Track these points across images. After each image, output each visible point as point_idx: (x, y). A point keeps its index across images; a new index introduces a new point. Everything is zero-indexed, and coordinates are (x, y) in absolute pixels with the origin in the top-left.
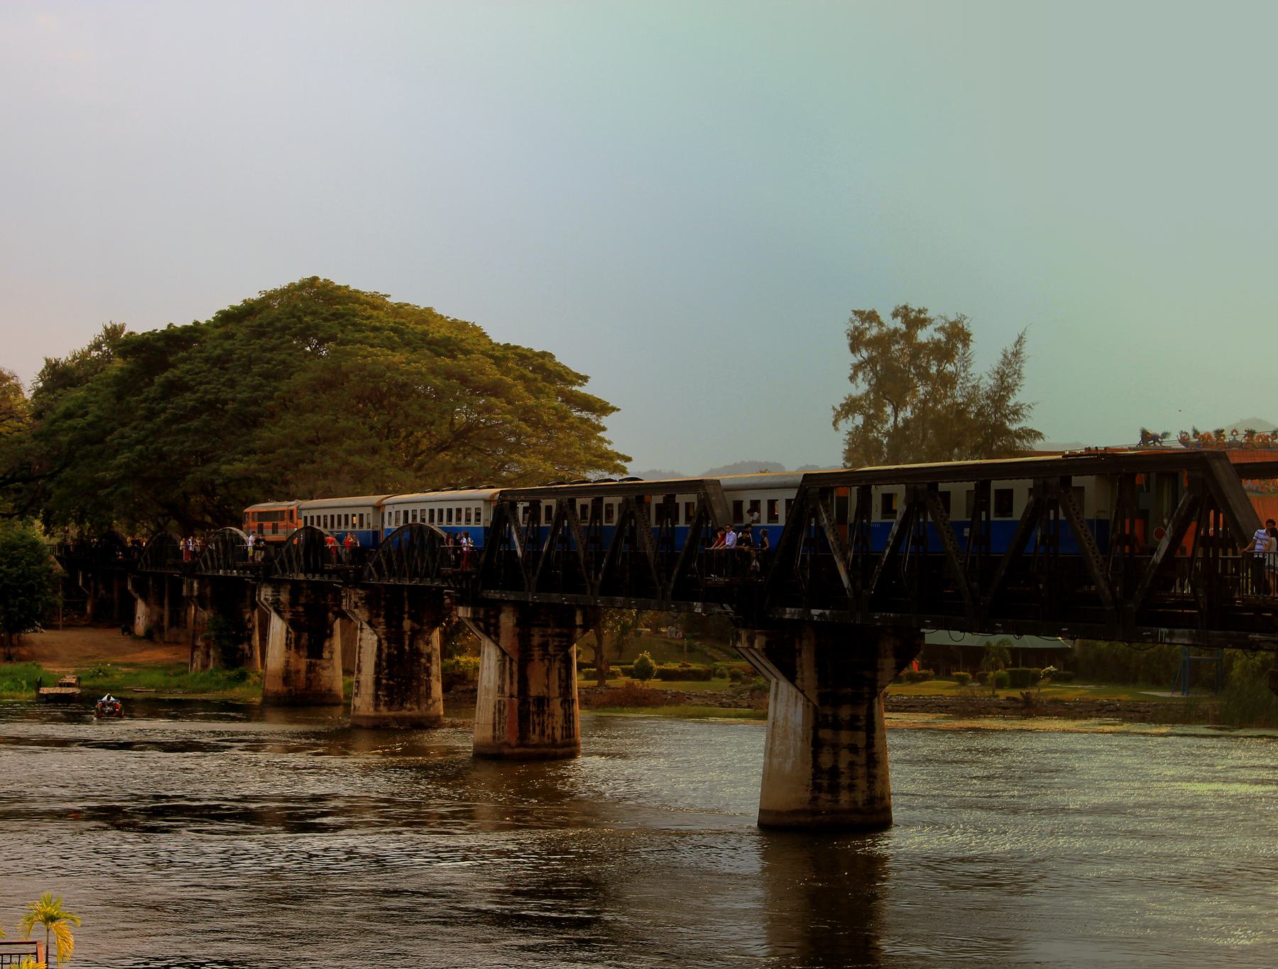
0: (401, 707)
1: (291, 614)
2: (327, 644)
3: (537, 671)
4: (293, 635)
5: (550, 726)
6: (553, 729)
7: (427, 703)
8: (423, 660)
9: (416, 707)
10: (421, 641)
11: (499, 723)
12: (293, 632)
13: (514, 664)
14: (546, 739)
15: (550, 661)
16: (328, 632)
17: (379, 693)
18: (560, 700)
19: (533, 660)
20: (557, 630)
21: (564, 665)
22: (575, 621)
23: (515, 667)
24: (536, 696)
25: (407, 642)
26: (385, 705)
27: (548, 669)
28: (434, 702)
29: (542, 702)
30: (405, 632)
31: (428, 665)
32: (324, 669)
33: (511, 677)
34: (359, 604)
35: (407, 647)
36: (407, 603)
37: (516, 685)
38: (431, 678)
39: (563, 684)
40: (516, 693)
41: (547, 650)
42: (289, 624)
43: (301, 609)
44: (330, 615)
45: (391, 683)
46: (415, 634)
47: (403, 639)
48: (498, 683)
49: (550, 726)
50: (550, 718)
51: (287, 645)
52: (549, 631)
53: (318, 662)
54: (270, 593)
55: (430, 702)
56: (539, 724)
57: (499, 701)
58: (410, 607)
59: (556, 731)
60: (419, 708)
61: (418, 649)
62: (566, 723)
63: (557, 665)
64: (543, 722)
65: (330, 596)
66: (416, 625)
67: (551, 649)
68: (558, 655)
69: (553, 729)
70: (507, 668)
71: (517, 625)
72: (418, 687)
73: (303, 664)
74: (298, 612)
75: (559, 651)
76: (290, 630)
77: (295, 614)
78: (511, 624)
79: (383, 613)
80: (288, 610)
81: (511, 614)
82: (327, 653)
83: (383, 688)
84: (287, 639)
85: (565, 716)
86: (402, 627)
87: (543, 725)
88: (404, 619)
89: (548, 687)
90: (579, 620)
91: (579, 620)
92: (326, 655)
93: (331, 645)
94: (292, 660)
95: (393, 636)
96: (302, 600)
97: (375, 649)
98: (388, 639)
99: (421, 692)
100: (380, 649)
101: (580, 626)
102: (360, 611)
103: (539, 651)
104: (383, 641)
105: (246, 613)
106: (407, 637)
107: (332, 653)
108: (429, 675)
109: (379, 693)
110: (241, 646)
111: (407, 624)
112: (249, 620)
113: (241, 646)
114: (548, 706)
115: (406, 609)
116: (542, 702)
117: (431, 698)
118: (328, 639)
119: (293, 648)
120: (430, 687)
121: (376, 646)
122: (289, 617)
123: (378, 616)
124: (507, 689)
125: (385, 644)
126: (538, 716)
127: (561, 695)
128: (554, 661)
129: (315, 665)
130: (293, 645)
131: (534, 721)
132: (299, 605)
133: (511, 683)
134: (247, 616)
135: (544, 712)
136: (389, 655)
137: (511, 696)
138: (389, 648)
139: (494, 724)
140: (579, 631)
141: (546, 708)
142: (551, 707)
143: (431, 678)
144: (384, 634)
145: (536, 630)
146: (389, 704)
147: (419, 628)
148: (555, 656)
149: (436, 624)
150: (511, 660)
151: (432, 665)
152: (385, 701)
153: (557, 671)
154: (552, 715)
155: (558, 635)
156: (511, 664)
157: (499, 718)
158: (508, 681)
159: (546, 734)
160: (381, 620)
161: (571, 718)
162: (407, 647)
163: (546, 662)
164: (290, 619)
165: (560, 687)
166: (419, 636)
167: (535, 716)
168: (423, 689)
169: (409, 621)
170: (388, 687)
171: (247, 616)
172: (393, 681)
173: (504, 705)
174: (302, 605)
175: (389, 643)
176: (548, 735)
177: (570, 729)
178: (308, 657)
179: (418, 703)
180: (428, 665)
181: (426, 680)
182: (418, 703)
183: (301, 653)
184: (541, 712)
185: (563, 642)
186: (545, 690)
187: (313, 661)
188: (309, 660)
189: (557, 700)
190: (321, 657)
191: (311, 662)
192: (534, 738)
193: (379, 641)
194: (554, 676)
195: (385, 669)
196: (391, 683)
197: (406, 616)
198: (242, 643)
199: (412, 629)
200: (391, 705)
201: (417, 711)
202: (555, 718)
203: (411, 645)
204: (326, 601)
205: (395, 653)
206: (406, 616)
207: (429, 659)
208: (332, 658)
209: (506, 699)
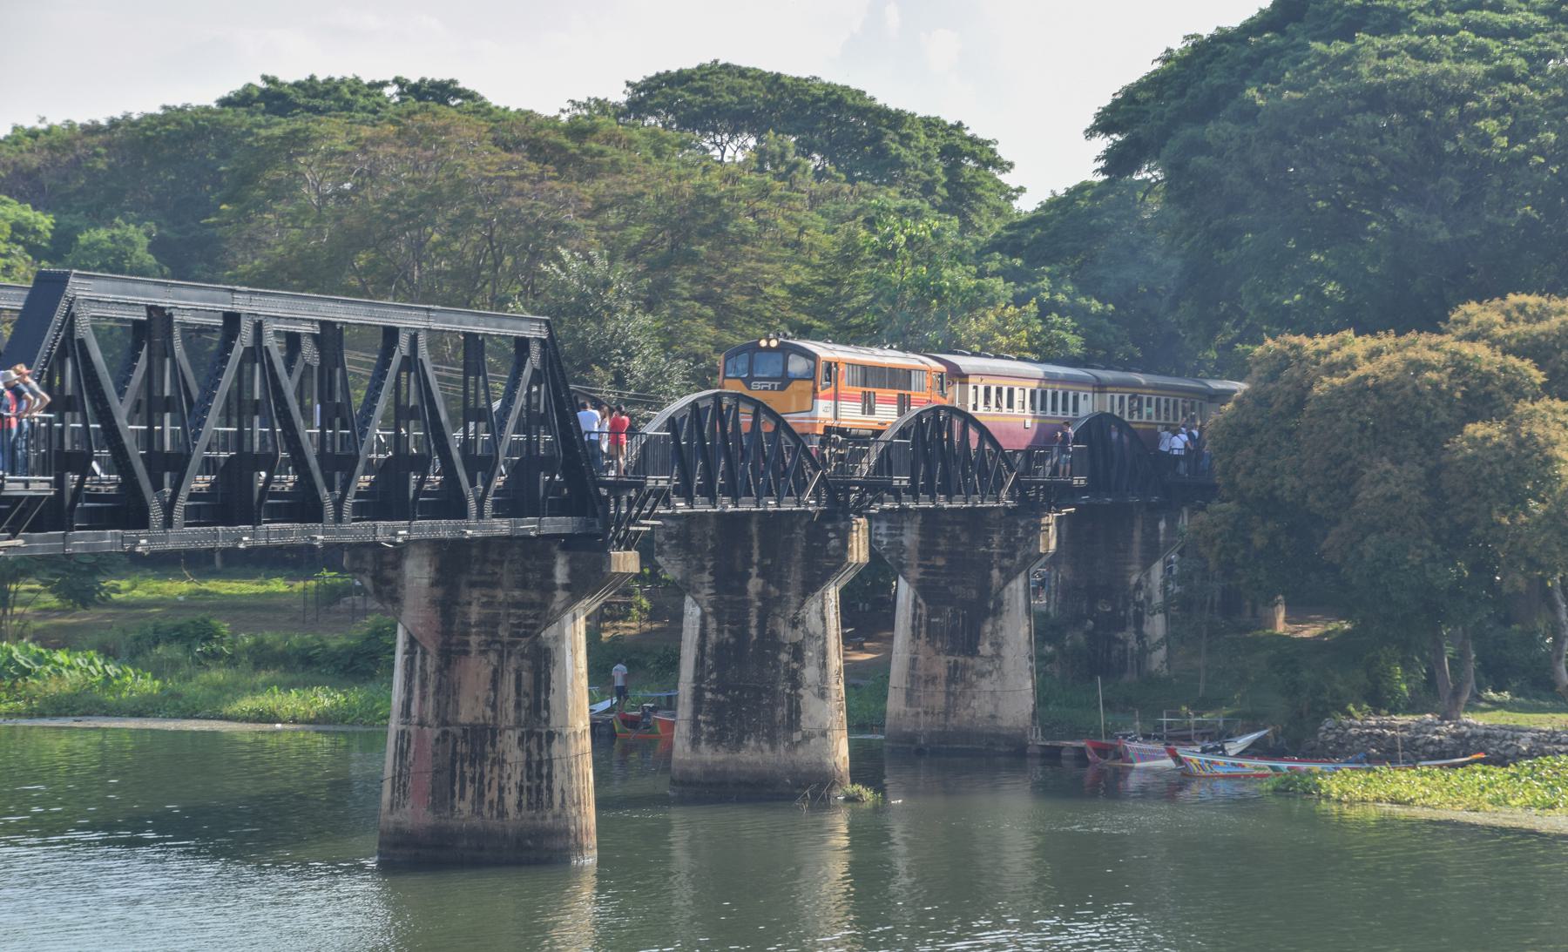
0: (738, 744)
1: (921, 570)
2: (988, 628)
3: (475, 671)
4: (924, 611)
5: (495, 784)
6: (501, 789)
7: (789, 739)
8: (784, 657)
9: (766, 747)
10: (780, 620)
11: (400, 776)
12: (924, 605)
13: (429, 659)
14: (485, 809)
15: (501, 656)
16: (991, 605)
17: (700, 717)
18: (518, 733)
19: (467, 653)
20: (517, 593)
21: (527, 663)
22: (551, 575)
23: (431, 666)
24: (471, 724)
25: (754, 621)
26: (708, 741)
27: (495, 671)
28: (807, 738)
29: (482, 736)
30: (751, 601)
31: (795, 665)
32: (982, 675)
33: (423, 685)
34: (665, 547)
35: (754, 632)
36: (756, 544)
37: (430, 703)
38: (801, 691)
39: (526, 702)
40: (430, 717)
41: (494, 634)
42: (917, 589)
43: (940, 562)
44: (995, 573)
45: (721, 697)
46: (770, 605)
47: (747, 614)
48: (403, 696)
49: (495, 784)
50: (496, 769)
51: (913, 628)
52: (500, 595)
53: (970, 661)
54: (883, 531)
55: (797, 736)
56: (473, 780)
57: (403, 732)
58: (763, 555)
59: (506, 794)
60: (773, 749)
61: (774, 634)
62: (529, 778)
63: (513, 663)
64: (482, 776)
65: (996, 538)
66: (772, 589)
67: (503, 633)
68: (518, 643)
69: (501, 789)
70: (418, 668)
71: (434, 584)
72: (772, 707)
73: (941, 666)
74: (933, 566)
75: (518, 635)
76: (920, 601)
77: (929, 570)
78: (425, 581)
79: (709, 564)
80: (915, 563)
81: (426, 563)
82: (987, 645)
83: (705, 707)
84: (914, 616)
85: (528, 764)
86: (745, 592)
87: (481, 782)
88: (749, 576)
89: (494, 707)
90: (561, 574)
91: (561, 574)
92: (986, 648)
93: (994, 632)
94: (921, 657)
95: (728, 607)
96: (943, 545)
97: (697, 632)
98: (718, 614)
99: (778, 718)
100: (703, 635)
101: (566, 587)
102: (669, 561)
103: (478, 634)
104: (710, 619)
105: (1132, 572)
106: (753, 612)
107: (997, 645)
108: (795, 680)
109: (700, 717)
110: (1120, 635)
111: (754, 585)
112: (1139, 586)
113: (1120, 635)
114: (493, 745)
115: (756, 558)
116: (482, 736)
117: (798, 728)
118: (991, 619)
119: (923, 635)
120: (798, 707)
121: (698, 626)
122: (918, 576)
123: (702, 569)
124: (414, 709)
125: (712, 624)
126: (472, 764)
127: (518, 724)
128: (509, 654)
129: (965, 667)
130: (923, 629)
131: (463, 773)
132: (937, 553)
133: (423, 698)
134: (1134, 579)
135: (484, 757)
136: (720, 647)
137: (422, 724)
138: (720, 631)
139: (393, 778)
140: (560, 596)
141: (488, 749)
142: (500, 746)
143: (801, 691)
144: (711, 604)
145: (476, 593)
146: (717, 739)
147: (777, 593)
148: (513, 644)
149: (812, 585)
150: (424, 653)
151: (803, 666)
152: (711, 735)
153: (513, 676)
154: (500, 762)
155: (517, 605)
156: (423, 659)
157: (400, 765)
158: (417, 692)
159: (487, 800)
160: (706, 577)
161: (545, 771)
162: (754, 632)
163: (493, 657)
164: (919, 581)
165: (518, 705)
166: (778, 611)
167: (466, 764)
168: (781, 712)
169: (761, 581)
170: (718, 709)
171: (1134, 579)
172: (724, 693)
173: (409, 741)
174: (942, 554)
175: (720, 622)
176: (491, 802)
177: (539, 791)
178: (951, 652)
179: (772, 741)
180: (795, 665)
181: (789, 695)
182: (772, 741)
183: (939, 645)
184: (477, 758)
185: (527, 617)
186: (489, 713)
187: (961, 660)
188: (952, 659)
189: (511, 732)
190: (972, 650)
191: (956, 662)
192: (464, 806)
193: (703, 617)
194: (508, 686)
195: (711, 672)
196: (721, 697)
197: (754, 571)
198: (1123, 629)
199: (763, 595)
200: (720, 741)
201: (768, 753)
202: (507, 769)
203: (762, 625)
204: (988, 546)
205: (732, 641)
206: (754, 571)
207: (798, 652)
208: (998, 656)
209: (412, 729)
